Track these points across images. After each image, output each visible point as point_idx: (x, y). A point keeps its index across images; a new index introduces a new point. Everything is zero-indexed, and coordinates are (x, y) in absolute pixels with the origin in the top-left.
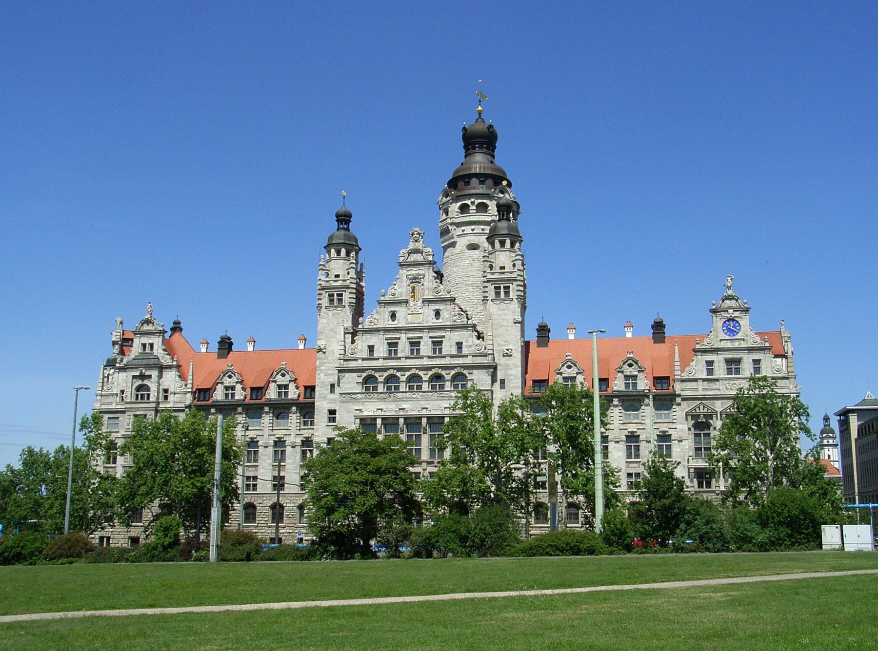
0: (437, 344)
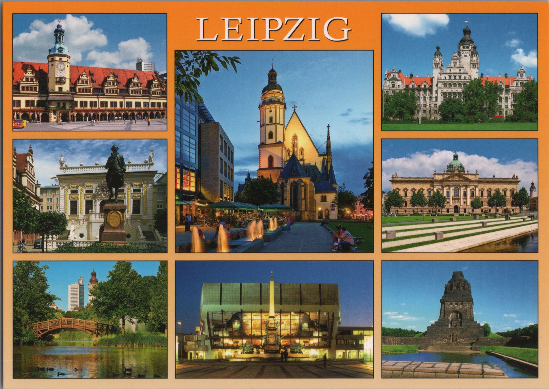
0: (460, 77)
